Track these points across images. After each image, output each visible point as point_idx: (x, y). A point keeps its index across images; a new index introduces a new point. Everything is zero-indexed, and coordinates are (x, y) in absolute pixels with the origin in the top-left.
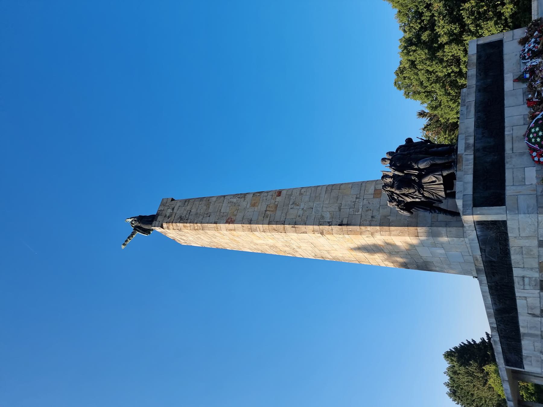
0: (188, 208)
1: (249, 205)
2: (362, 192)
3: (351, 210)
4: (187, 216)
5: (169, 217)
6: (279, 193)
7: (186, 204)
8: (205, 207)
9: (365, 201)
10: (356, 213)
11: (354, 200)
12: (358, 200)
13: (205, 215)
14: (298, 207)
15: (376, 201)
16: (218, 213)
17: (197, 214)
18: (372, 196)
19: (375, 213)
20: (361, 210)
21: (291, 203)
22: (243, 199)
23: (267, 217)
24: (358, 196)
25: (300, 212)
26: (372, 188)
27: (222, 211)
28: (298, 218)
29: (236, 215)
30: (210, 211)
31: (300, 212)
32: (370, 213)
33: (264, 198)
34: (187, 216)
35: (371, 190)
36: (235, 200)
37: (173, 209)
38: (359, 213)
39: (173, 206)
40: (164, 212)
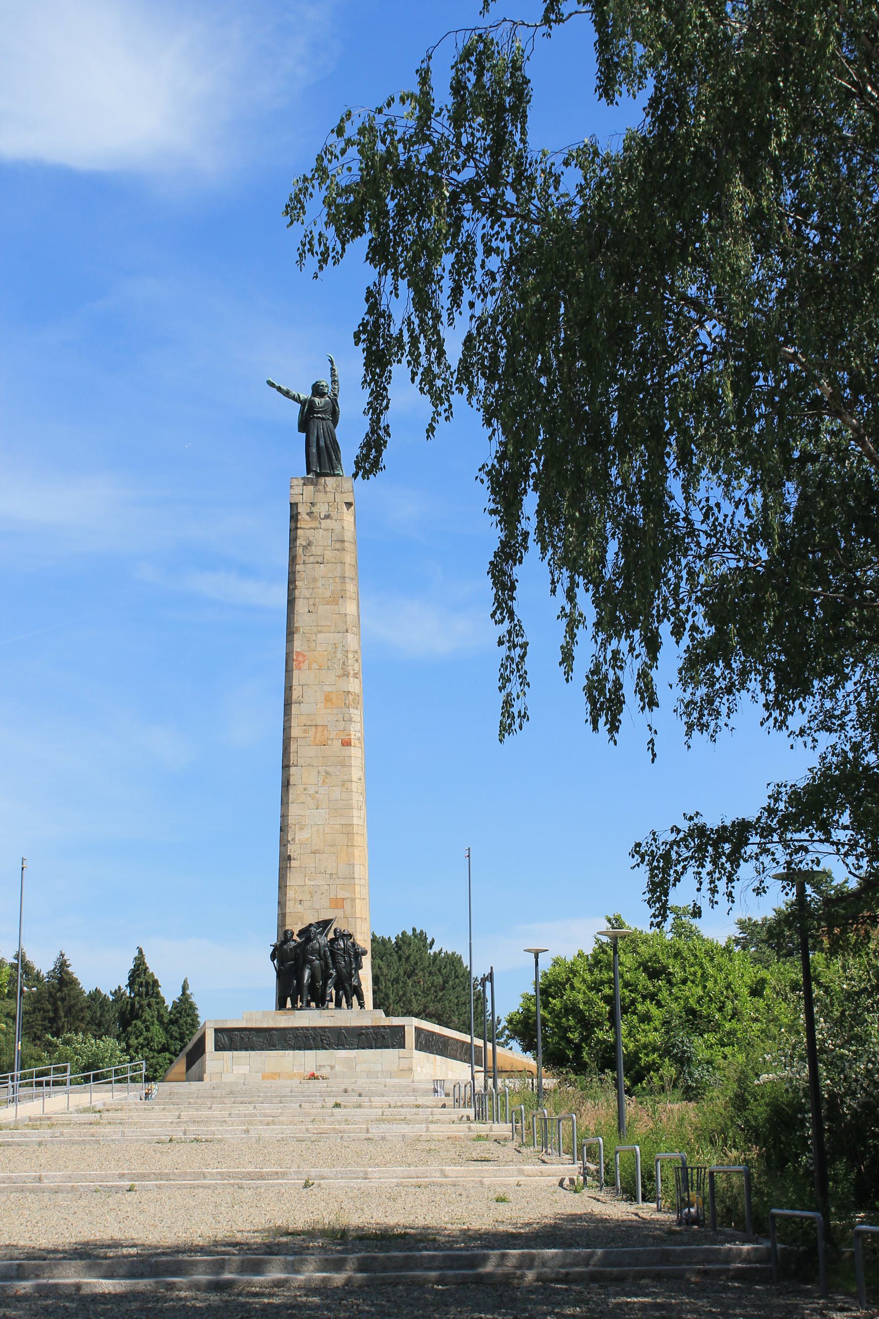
0: (329, 555)
1: (328, 689)
2: (341, 881)
3: (313, 870)
4: (312, 559)
5: (310, 514)
6: (347, 743)
7: (338, 545)
8: (328, 593)
13: (311, 602)
14: (320, 784)
15: (326, 903)
16: (315, 629)
17: (315, 580)
19: (307, 904)
20: (312, 883)
21: (328, 769)
22: (340, 672)
23: (305, 732)
25: (312, 790)
26: (346, 895)
27: (319, 635)
28: (301, 787)
29: (310, 668)
30: (320, 607)
31: (312, 790)
32: (308, 897)
33: (340, 716)
34: (312, 559)
35: (341, 894)
36: (339, 655)
37: (327, 517)
38: (307, 882)
39: (334, 514)
40: (321, 495)
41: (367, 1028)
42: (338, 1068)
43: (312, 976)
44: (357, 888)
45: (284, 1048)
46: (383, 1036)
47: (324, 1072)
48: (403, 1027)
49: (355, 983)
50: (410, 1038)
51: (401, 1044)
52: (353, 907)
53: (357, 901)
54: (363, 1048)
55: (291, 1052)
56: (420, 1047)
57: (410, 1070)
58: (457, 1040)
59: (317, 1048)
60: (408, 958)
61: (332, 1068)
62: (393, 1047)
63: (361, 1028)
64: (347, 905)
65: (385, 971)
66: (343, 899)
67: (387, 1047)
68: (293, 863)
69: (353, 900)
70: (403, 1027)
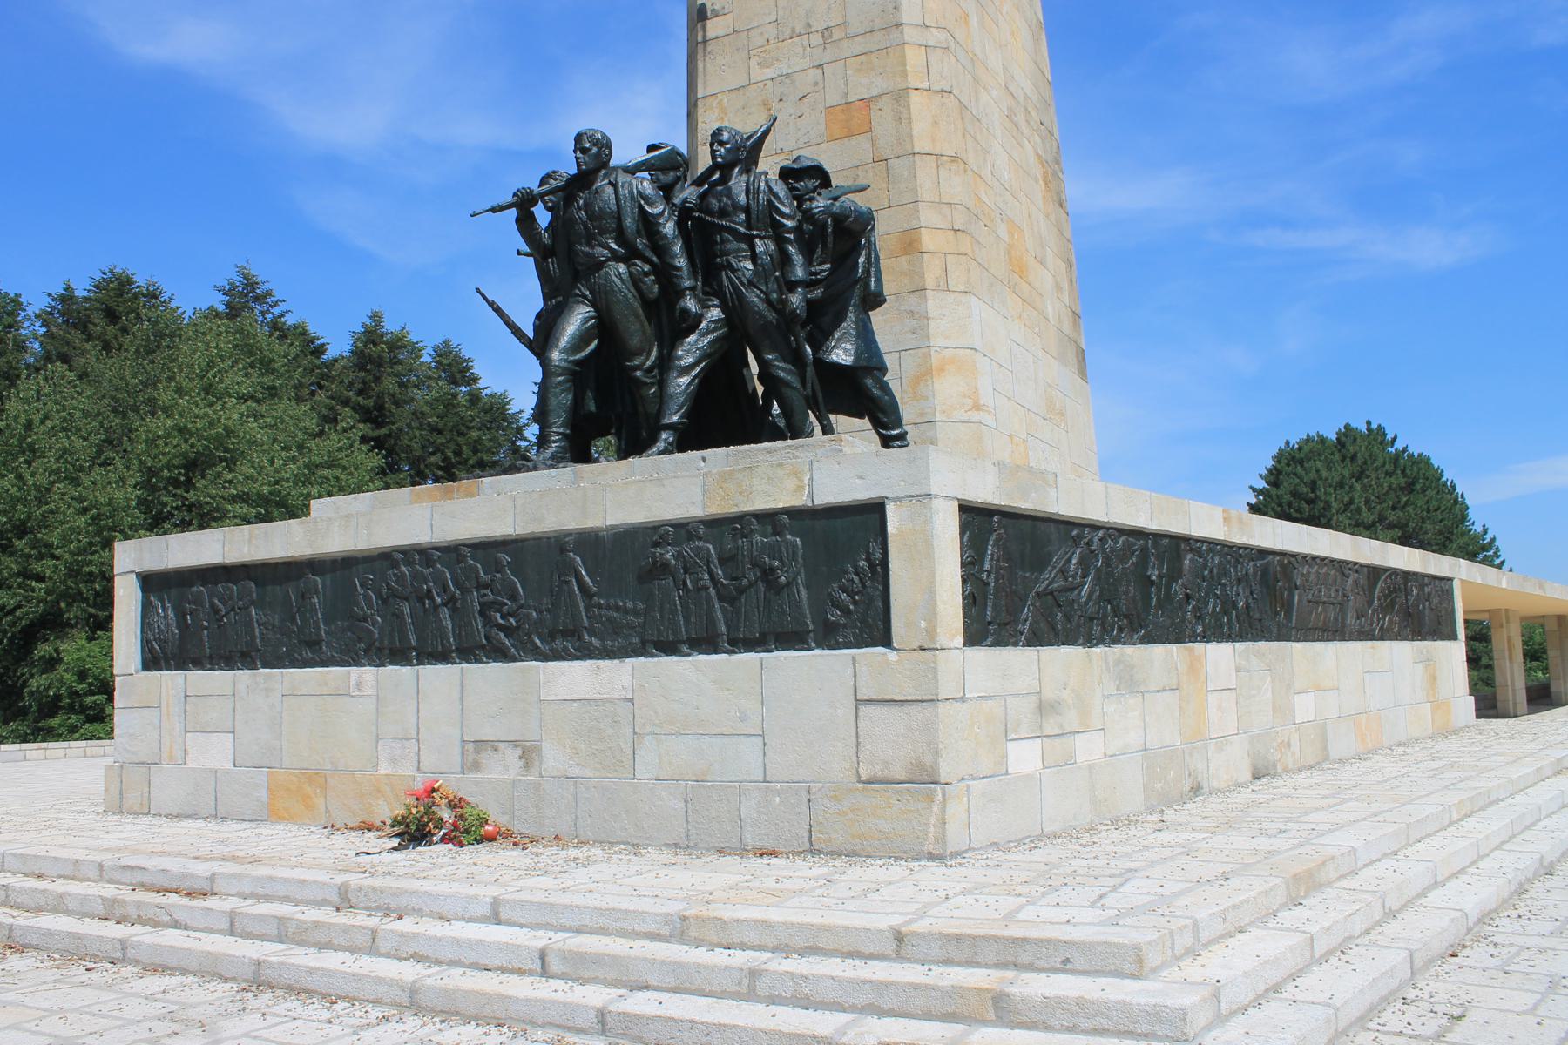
2: (858, 46)
3: (771, 31)
9: (815, 74)
10: (754, 61)
11: (818, 25)
12: (816, 39)
18: (834, 98)
20: (769, 73)
24: (837, 34)
26: (878, 85)
41: (684, 530)
42: (554, 758)
43: (604, 328)
44: (914, 58)
45: (349, 658)
46: (768, 574)
47: (487, 788)
48: (874, 511)
49: (842, 355)
50: (929, 573)
51: (862, 617)
52: (902, 118)
53: (915, 99)
54: (669, 648)
55: (365, 676)
56: (993, 618)
57: (925, 778)
58: (1342, 567)
59: (468, 652)
60: (1354, 457)
61: (529, 754)
62: (829, 637)
63: (655, 534)
64: (882, 118)
65: (1324, 474)
66: (867, 102)
67: (793, 639)
68: (714, 27)
69: (900, 96)
70: (874, 511)
